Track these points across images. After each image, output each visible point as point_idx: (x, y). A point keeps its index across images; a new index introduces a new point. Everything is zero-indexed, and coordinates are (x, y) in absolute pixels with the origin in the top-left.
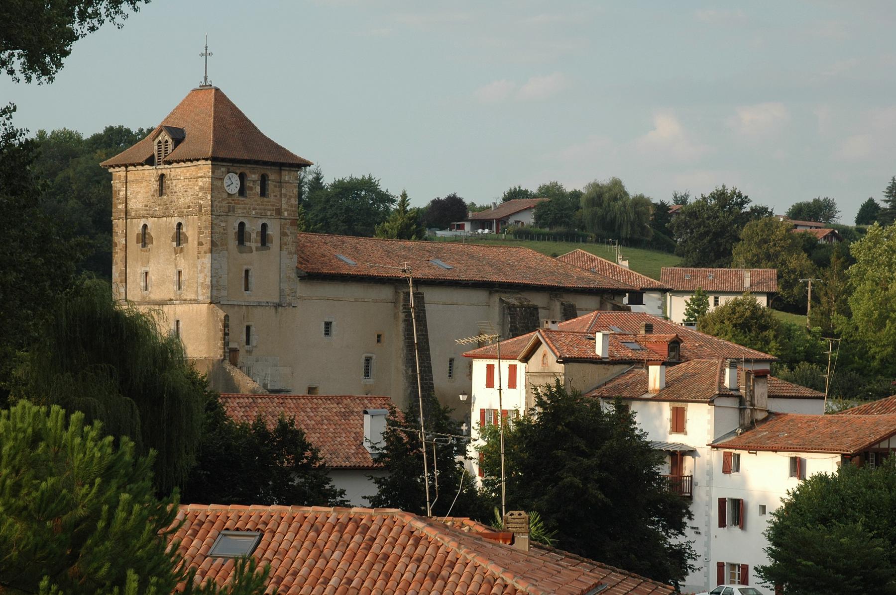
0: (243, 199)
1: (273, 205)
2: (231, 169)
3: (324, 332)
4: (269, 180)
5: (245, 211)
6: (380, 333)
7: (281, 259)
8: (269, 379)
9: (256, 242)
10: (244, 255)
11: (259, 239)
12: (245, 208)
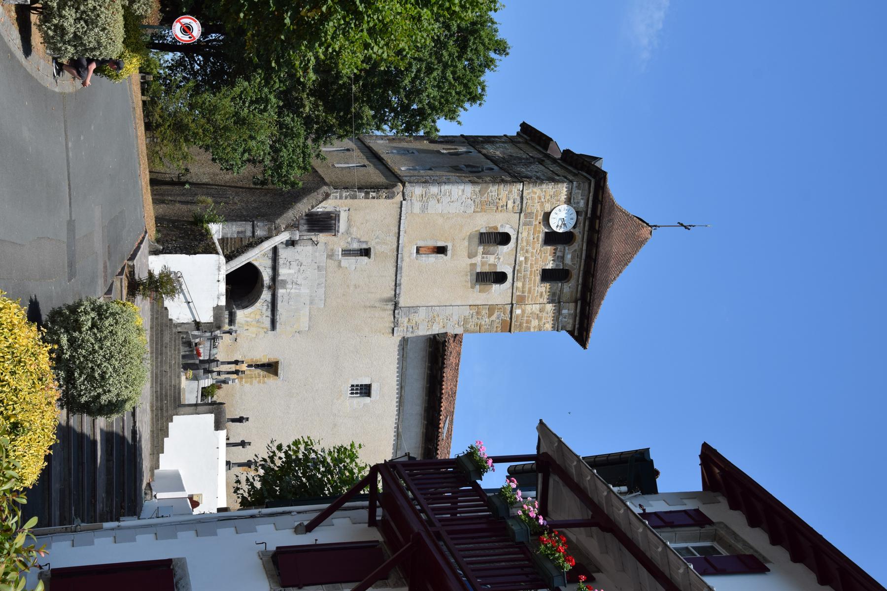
0: (540, 240)
1: (530, 292)
2: (581, 218)
3: (355, 383)
4: (562, 283)
5: (525, 244)
7: (459, 306)
8: (293, 291)
9: (483, 264)
10: (466, 244)
11: (486, 269)
12: (528, 243)
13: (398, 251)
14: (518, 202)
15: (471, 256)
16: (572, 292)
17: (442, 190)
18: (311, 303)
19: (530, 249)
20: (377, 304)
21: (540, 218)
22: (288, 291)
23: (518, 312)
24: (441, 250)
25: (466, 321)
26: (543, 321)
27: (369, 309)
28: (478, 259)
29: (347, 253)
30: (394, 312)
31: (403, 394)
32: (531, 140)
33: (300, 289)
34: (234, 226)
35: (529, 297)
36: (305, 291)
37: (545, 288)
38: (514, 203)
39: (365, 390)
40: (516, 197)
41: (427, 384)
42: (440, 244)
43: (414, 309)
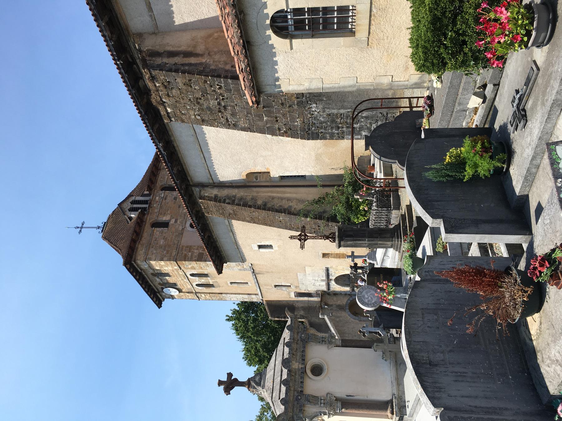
5: (187, 284)
30: (253, 270)
36: (310, 278)
41: (221, 250)
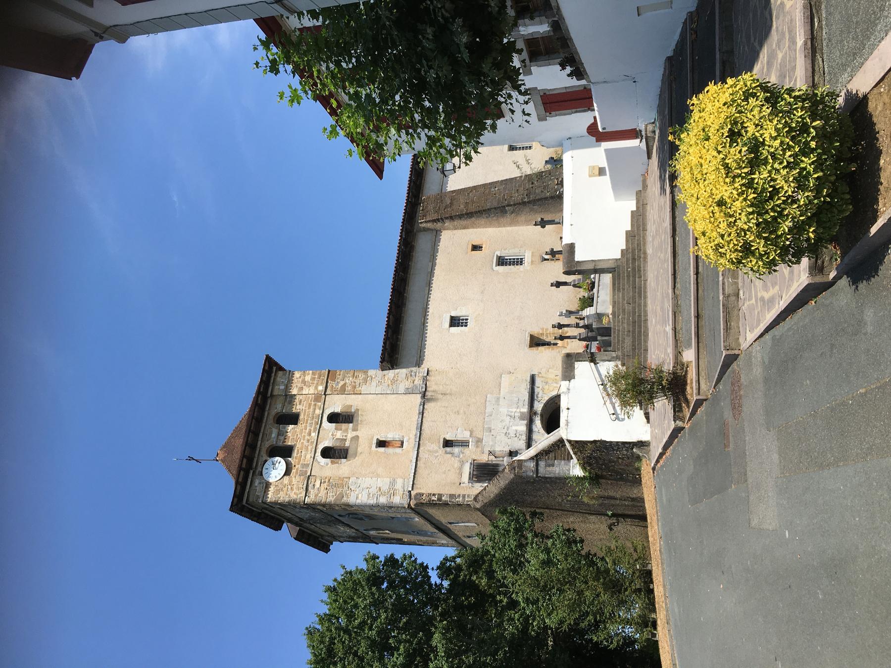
0: (296, 451)
1: (310, 405)
2: (259, 469)
3: (464, 328)
5: (310, 448)
6: (470, 247)
7: (370, 394)
8: (514, 410)
9: (346, 430)
10: (359, 450)
11: (344, 426)
13: (419, 444)
14: (310, 486)
15: (356, 438)
16: (275, 404)
17: (375, 499)
18: (498, 399)
19: (306, 443)
20: (440, 396)
21: (294, 471)
22: (518, 410)
23: (321, 388)
24: (382, 444)
25: (365, 381)
26: (300, 380)
27: (448, 392)
28: (351, 434)
29: (464, 444)
30: (426, 389)
31: (423, 319)
32: (318, 538)
33: (508, 411)
34: (557, 472)
35: (311, 401)
36: (504, 410)
37: (297, 408)
38: (314, 485)
39: (455, 322)
40: (312, 491)
41: (402, 327)
42: (382, 450)
43: (408, 392)
